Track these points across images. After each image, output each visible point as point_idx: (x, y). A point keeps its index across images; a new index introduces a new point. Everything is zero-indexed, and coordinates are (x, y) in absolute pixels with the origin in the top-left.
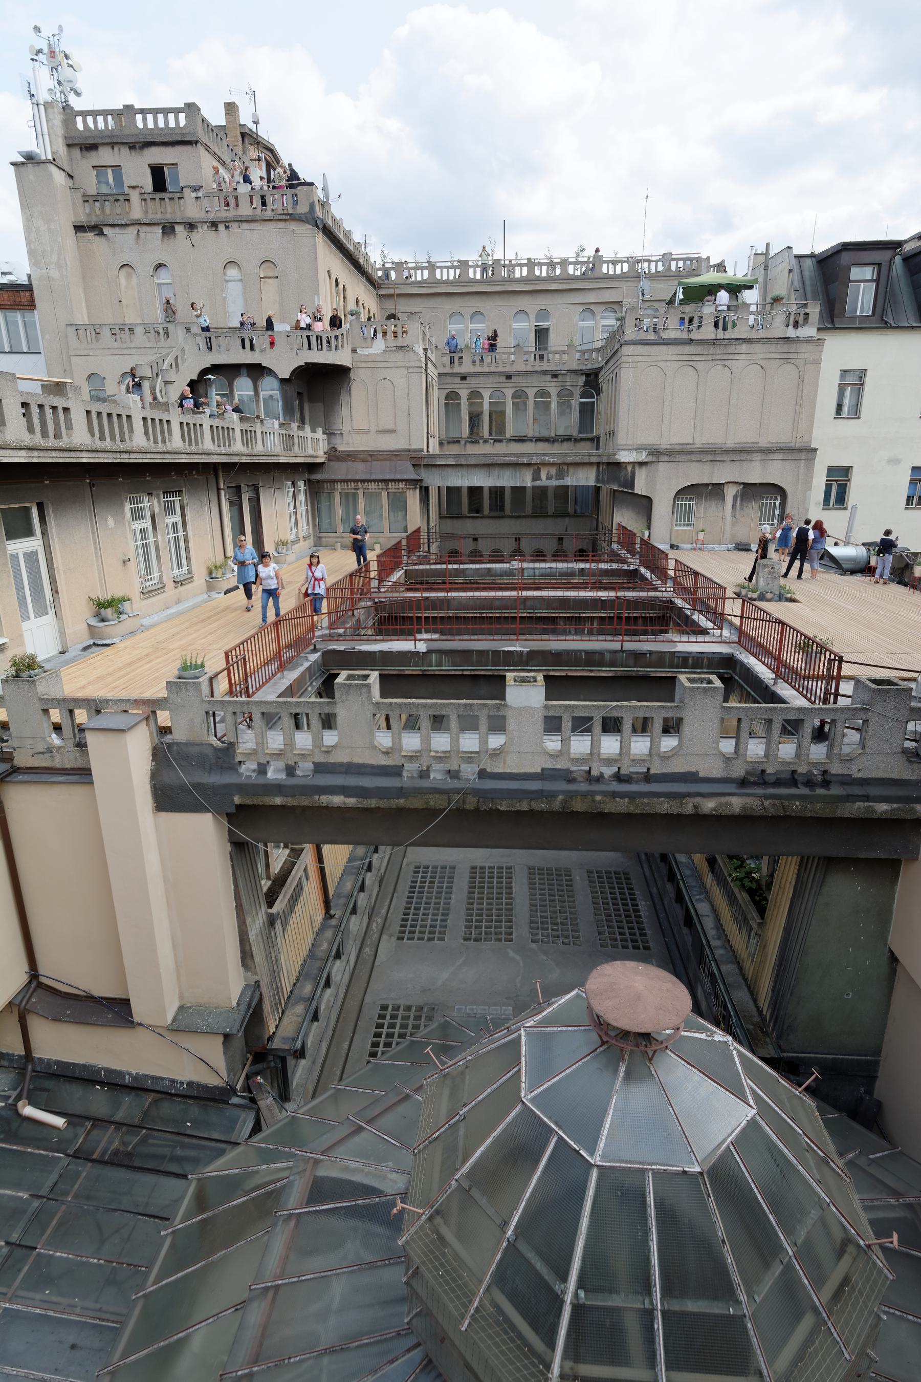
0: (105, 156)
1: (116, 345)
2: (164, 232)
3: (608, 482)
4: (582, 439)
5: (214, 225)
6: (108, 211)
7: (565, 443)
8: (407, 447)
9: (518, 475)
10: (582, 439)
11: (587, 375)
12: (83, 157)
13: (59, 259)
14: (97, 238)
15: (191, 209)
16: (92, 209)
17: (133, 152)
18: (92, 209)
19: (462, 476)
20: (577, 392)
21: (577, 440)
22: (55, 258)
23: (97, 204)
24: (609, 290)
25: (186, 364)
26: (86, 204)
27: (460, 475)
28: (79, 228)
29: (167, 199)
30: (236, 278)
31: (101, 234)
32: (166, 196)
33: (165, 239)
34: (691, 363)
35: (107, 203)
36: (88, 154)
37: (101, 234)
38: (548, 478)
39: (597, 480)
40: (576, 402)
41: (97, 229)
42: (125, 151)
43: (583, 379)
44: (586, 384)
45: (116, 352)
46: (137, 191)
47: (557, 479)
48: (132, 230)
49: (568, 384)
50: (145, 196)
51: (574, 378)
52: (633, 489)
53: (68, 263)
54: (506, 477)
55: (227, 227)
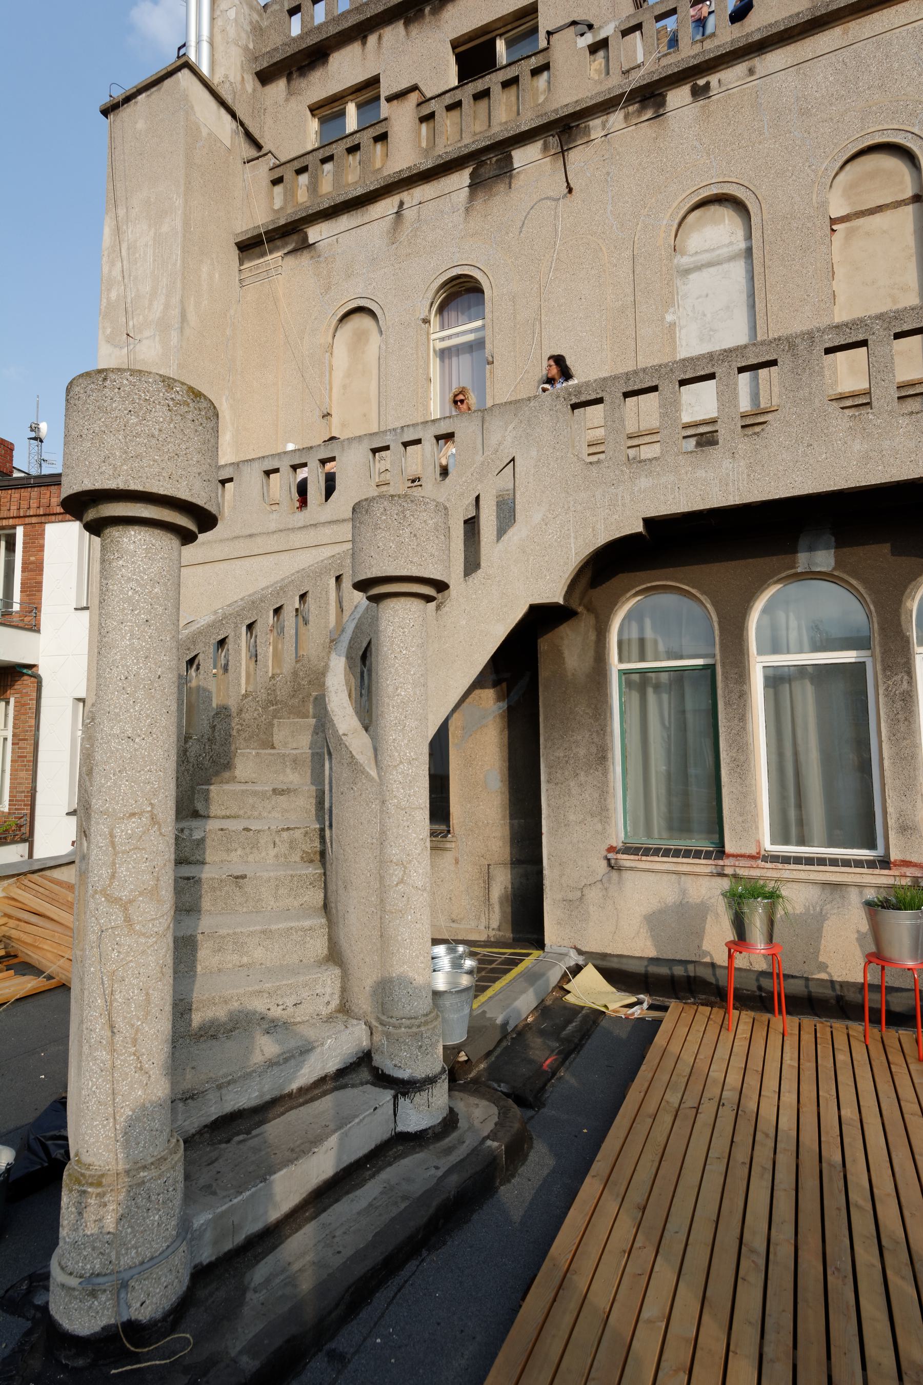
0: (345, 68)
1: (273, 521)
2: (475, 185)
5: (649, 96)
6: (326, 186)
12: (290, 93)
13: (167, 306)
14: (291, 261)
15: (575, 79)
16: (290, 195)
17: (415, 30)
18: (290, 195)
22: (158, 307)
23: (304, 179)
25: (515, 534)
26: (278, 189)
28: (250, 247)
29: (496, 90)
30: (724, 252)
31: (305, 246)
32: (493, 81)
33: (478, 203)
35: (328, 167)
36: (301, 83)
37: (305, 246)
41: (289, 234)
42: (394, 33)
45: (273, 543)
46: (414, 97)
48: (386, 207)
50: (433, 106)
53: (192, 317)
55: (699, 93)
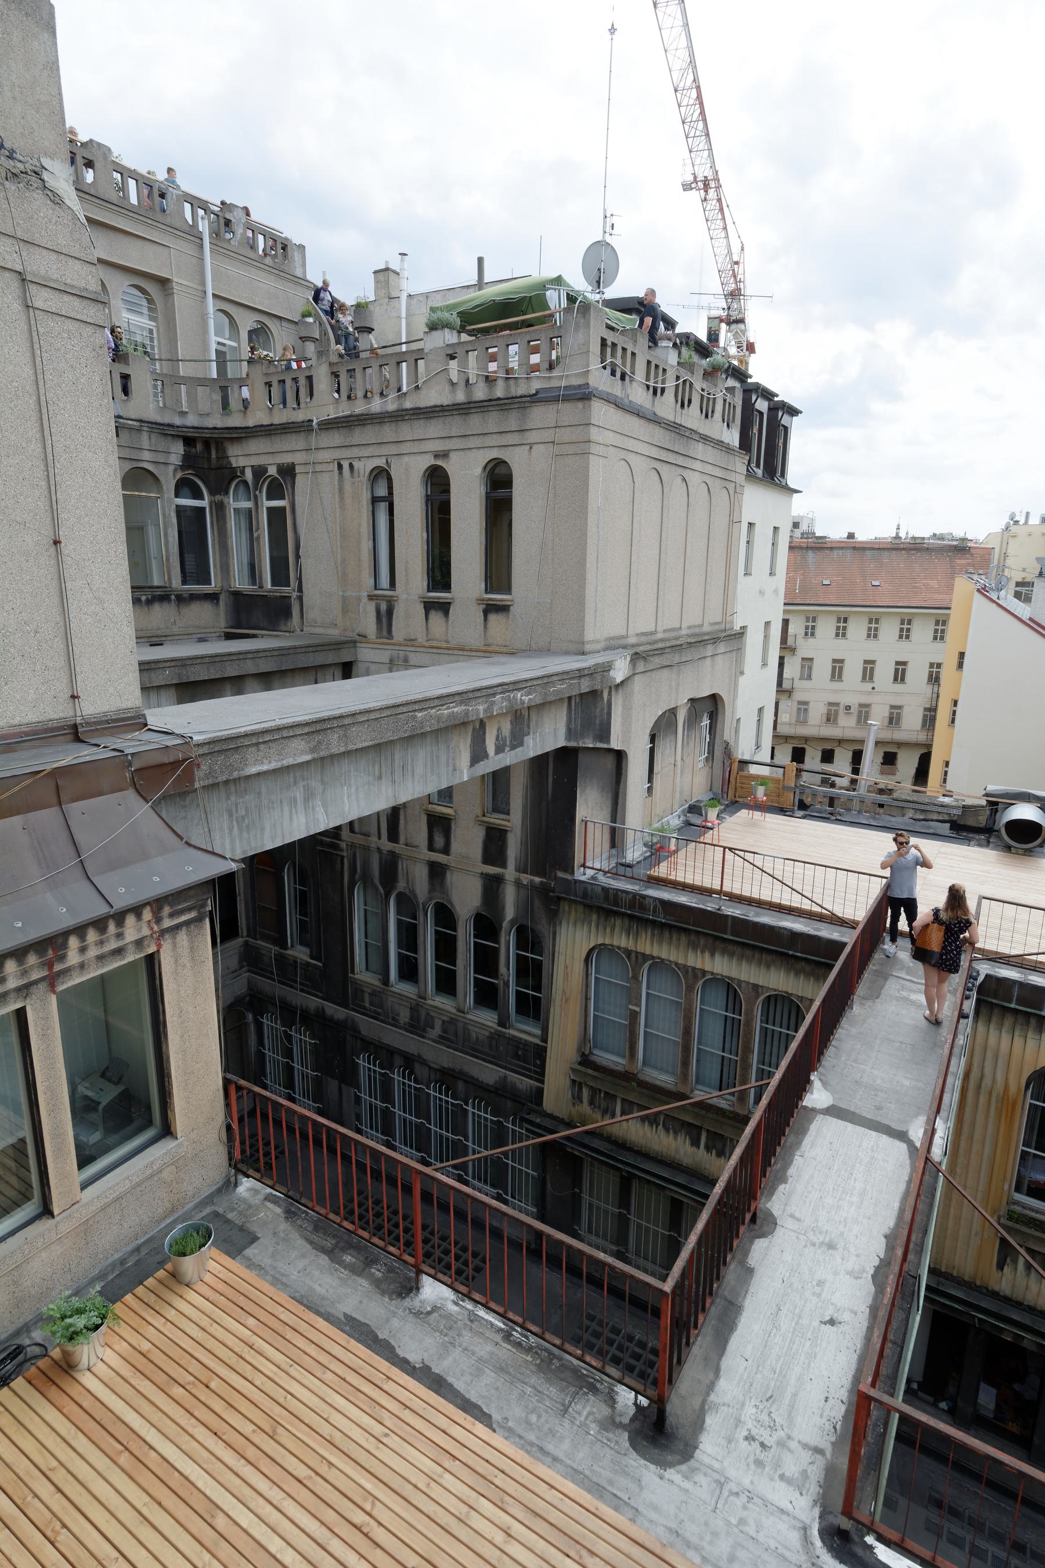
3: (583, 736)
4: (194, 597)
7: (156, 607)
8: (57, 711)
9: (443, 759)
10: (194, 597)
11: (189, 441)
19: (309, 796)
20: (169, 480)
21: (182, 600)
24: (139, 243)
27: (299, 793)
34: (658, 465)
38: (499, 750)
39: (570, 733)
40: (168, 503)
43: (177, 451)
44: (188, 461)
47: (513, 747)
49: (147, 456)
51: (162, 444)
52: (608, 742)
54: (419, 770)
